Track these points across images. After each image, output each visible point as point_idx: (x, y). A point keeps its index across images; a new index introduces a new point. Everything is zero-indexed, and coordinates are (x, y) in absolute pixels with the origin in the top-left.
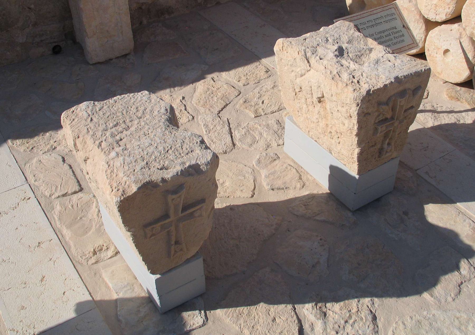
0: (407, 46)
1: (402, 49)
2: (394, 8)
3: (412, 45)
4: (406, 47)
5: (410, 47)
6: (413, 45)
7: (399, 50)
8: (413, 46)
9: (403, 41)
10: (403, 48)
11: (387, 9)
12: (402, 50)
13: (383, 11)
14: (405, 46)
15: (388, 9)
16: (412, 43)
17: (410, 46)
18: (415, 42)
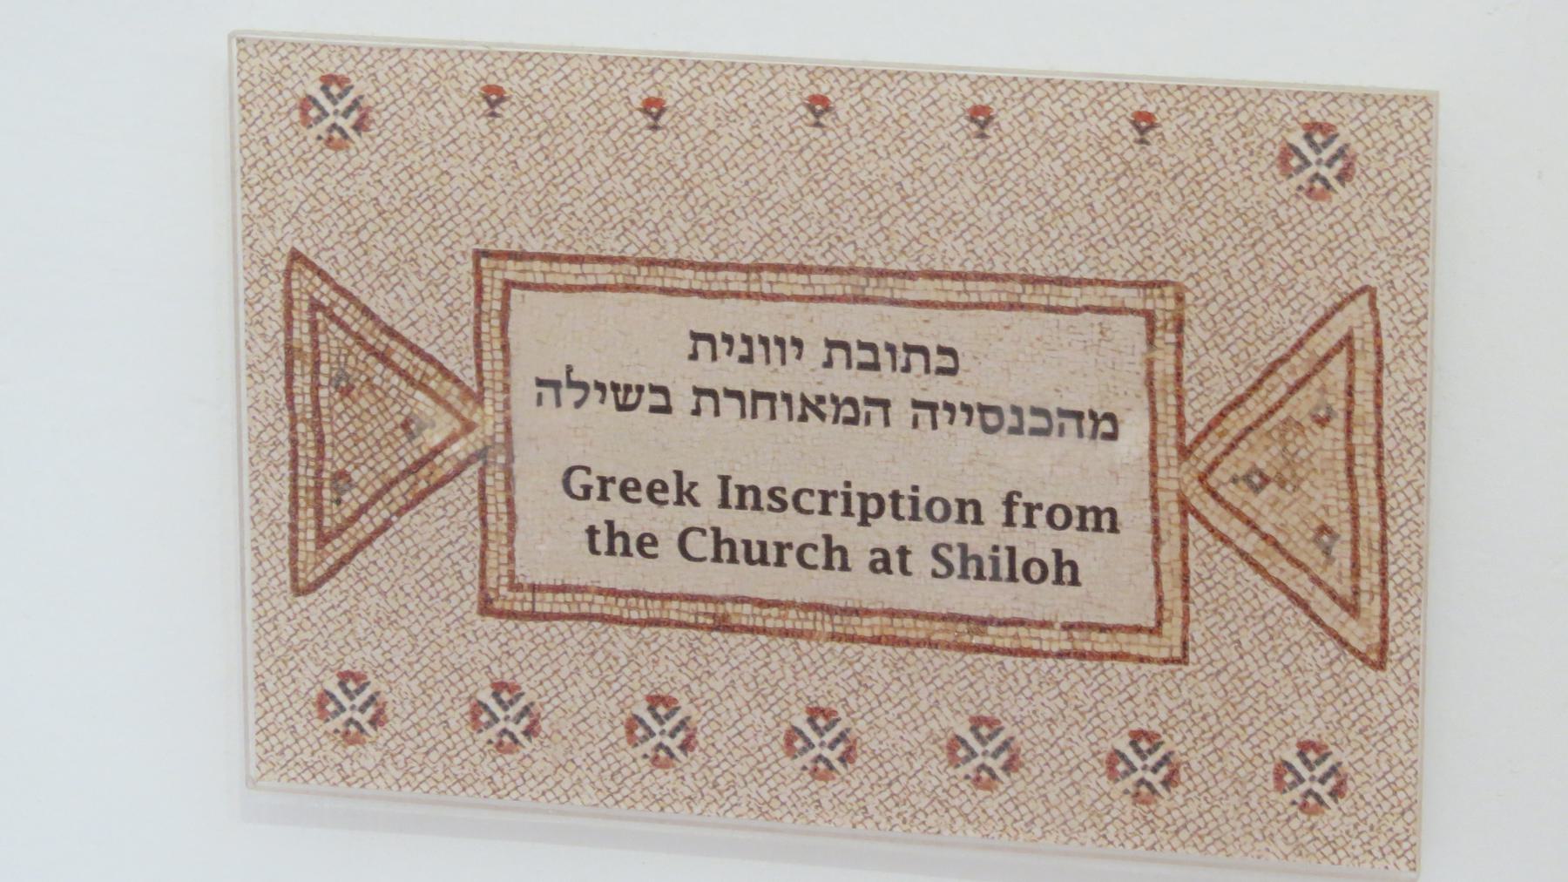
0: (1067, 627)
1: (992, 630)
2: (1149, 317)
3: (1122, 637)
4: (1044, 633)
5: (1087, 647)
6: (1141, 645)
7: (962, 627)
8: (1134, 651)
9: (1065, 571)
10: (1012, 630)
11: (1071, 303)
12: (987, 641)
13: (1011, 307)
14: (1044, 625)
15: (1076, 311)
16: (1138, 629)
17: (1103, 637)
18: (1172, 629)
